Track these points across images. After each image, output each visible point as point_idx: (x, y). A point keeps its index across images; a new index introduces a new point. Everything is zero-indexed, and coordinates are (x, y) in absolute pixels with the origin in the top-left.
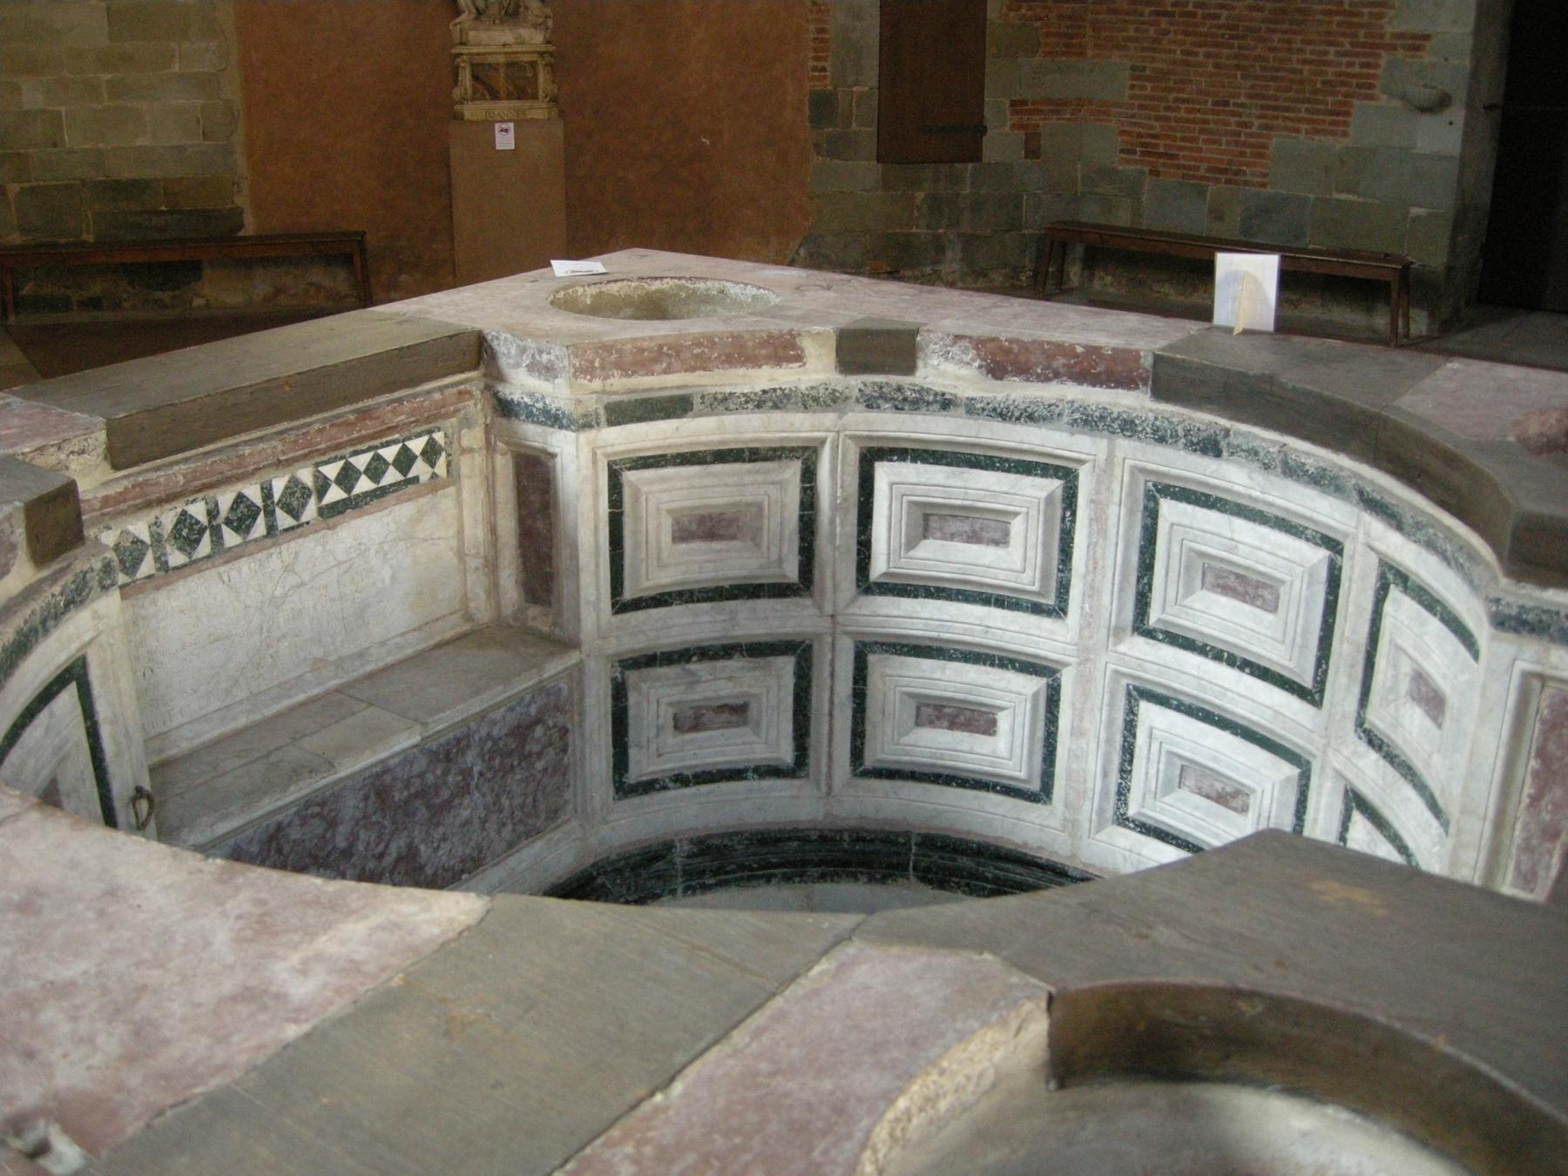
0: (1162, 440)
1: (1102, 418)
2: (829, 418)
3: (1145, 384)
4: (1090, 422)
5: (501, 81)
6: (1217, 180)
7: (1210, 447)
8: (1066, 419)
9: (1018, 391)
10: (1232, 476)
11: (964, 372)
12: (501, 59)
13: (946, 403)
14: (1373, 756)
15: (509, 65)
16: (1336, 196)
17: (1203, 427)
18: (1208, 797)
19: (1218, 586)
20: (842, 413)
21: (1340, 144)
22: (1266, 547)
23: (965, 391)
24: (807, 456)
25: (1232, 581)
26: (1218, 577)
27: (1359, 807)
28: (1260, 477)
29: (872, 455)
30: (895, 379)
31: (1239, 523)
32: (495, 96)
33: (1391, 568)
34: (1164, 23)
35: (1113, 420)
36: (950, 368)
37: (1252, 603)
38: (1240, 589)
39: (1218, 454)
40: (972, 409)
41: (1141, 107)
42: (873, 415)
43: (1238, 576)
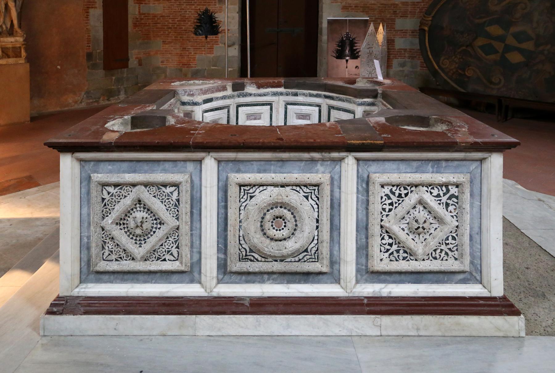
0: (287, 95)
2: (232, 100)
4: (275, 94)
5: (10, 53)
6: (184, 67)
7: (296, 95)
9: (262, 91)
10: (300, 99)
11: (253, 89)
12: (11, 46)
13: (250, 95)
15: (13, 48)
16: (212, 68)
20: (234, 99)
21: (212, 56)
23: (253, 92)
24: (228, 107)
25: (301, 117)
28: (305, 98)
29: (238, 106)
30: (242, 92)
32: (9, 57)
34: (170, 30)
36: (251, 88)
39: (297, 96)
40: (255, 95)
41: (166, 51)
42: (239, 99)
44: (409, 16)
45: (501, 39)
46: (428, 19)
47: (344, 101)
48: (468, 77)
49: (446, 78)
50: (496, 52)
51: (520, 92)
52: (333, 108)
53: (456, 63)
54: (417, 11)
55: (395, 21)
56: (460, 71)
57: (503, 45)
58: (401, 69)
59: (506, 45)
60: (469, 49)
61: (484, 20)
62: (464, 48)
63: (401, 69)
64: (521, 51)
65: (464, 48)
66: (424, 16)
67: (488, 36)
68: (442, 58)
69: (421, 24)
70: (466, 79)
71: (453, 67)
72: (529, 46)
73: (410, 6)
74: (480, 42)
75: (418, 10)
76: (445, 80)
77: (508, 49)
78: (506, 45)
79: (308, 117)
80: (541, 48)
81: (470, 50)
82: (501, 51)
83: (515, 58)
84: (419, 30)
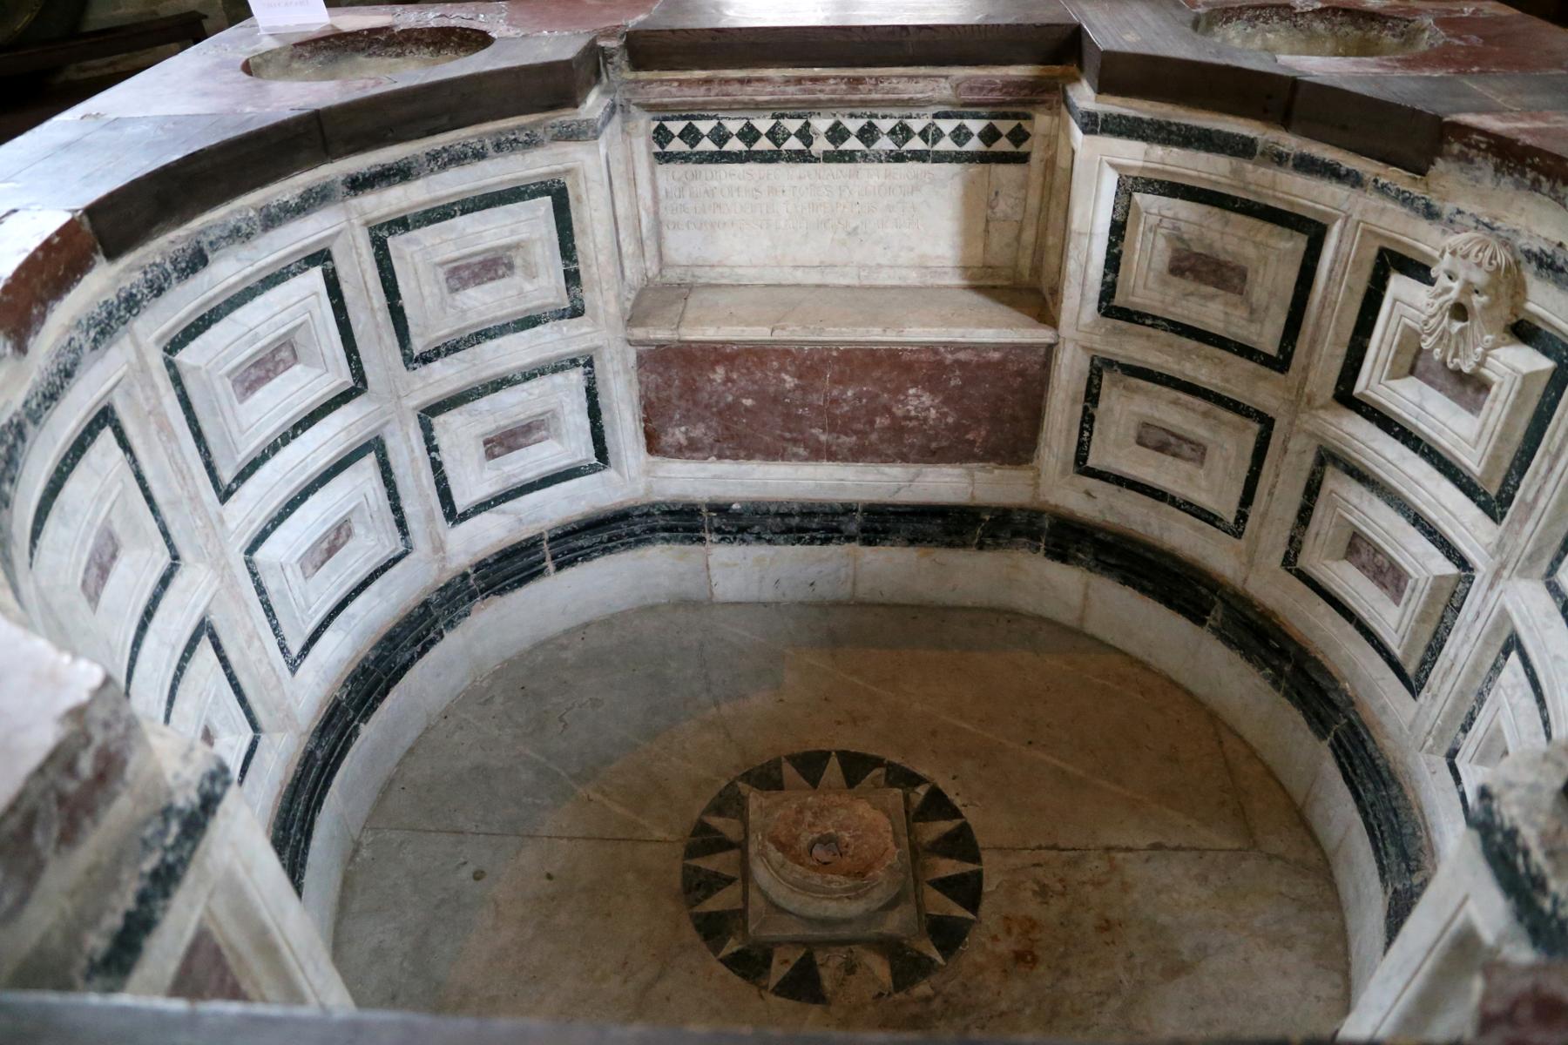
1: (110, 314)
3: (97, 253)
4: (106, 326)
7: (196, 261)
8: (87, 347)
10: (226, 272)
14: (436, 365)
17: (185, 245)
18: (323, 563)
19: (247, 389)
22: (277, 309)
25: (255, 373)
26: (243, 382)
27: (434, 415)
28: (244, 251)
31: (238, 314)
33: (381, 227)
35: (118, 309)
37: (276, 375)
38: (262, 373)
39: (204, 261)
43: (255, 365)
47: (480, 155)
52: (402, 224)
79: (285, 354)
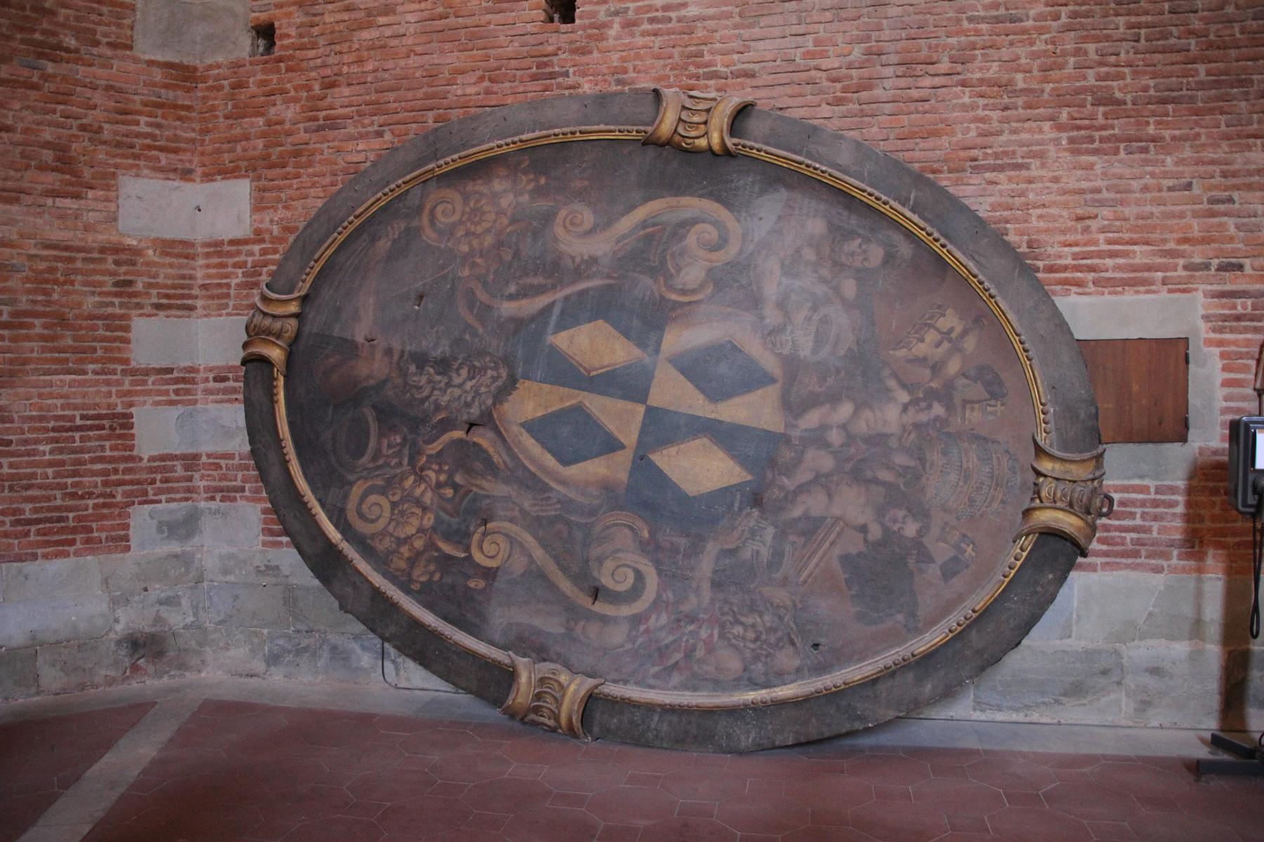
44: (199, 303)
45: (626, 383)
46: (279, 311)
48: (489, 574)
49: (377, 579)
50: (612, 446)
51: (738, 630)
53: (425, 509)
54: (234, 282)
55: (127, 329)
56: (446, 548)
57: (641, 409)
58: (175, 547)
59: (650, 410)
60: (483, 438)
61: (542, 301)
62: (458, 434)
63: (175, 547)
64: (726, 437)
65: (458, 434)
66: (265, 299)
67: (565, 372)
68: (357, 491)
69: (255, 333)
70: (476, 584)
71: (410, 530)
72: (755, 410)
73: (201, 262)
74: (529, 402)
75: (238, 278)
76: (377, 593)
77: (663, 428)
78: (650, 410)
80: (812, 419)
81: (484, 443)
82: (630, 437)
83: (701, 469)
84: (245, 362)
